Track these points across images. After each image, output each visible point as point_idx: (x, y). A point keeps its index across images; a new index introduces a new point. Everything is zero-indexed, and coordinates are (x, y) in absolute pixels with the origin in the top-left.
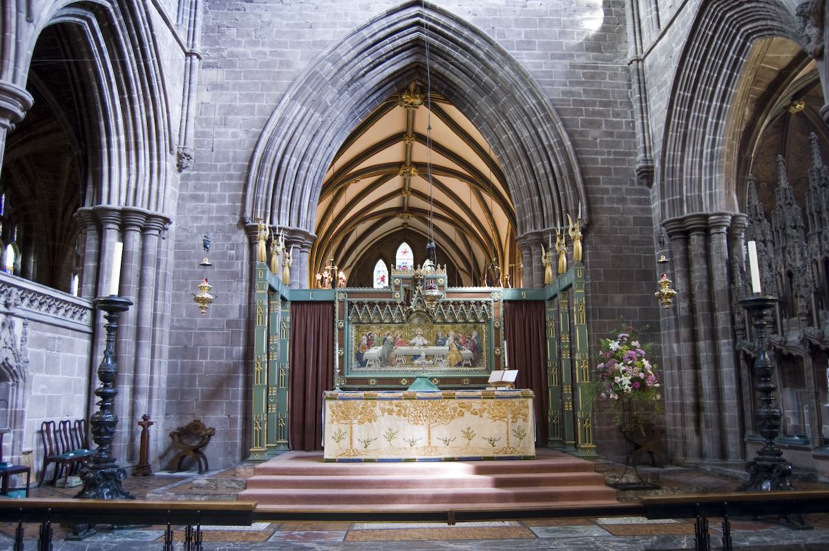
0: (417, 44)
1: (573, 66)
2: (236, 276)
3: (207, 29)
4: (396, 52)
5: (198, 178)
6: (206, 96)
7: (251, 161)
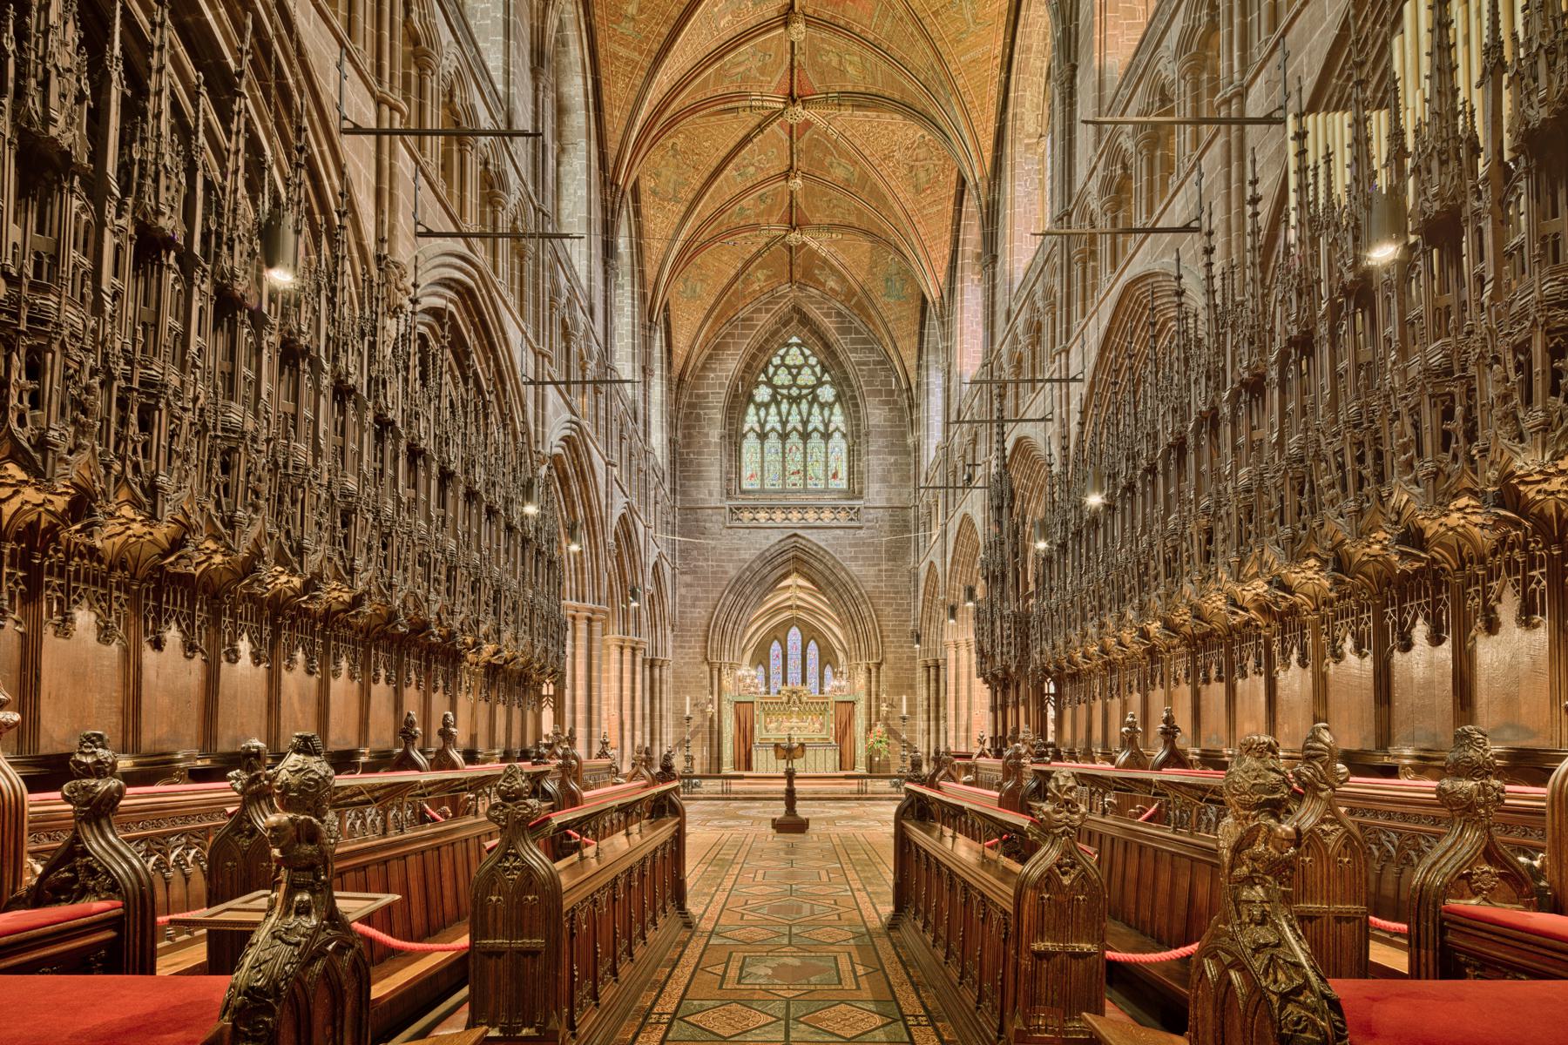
0: (795, 557)
1: (880, 571)
2: (703, 687)
3: (681, 551)
4: (784, 563)
5: (682, 636)
6: (683, 591)
7: (709, 627)
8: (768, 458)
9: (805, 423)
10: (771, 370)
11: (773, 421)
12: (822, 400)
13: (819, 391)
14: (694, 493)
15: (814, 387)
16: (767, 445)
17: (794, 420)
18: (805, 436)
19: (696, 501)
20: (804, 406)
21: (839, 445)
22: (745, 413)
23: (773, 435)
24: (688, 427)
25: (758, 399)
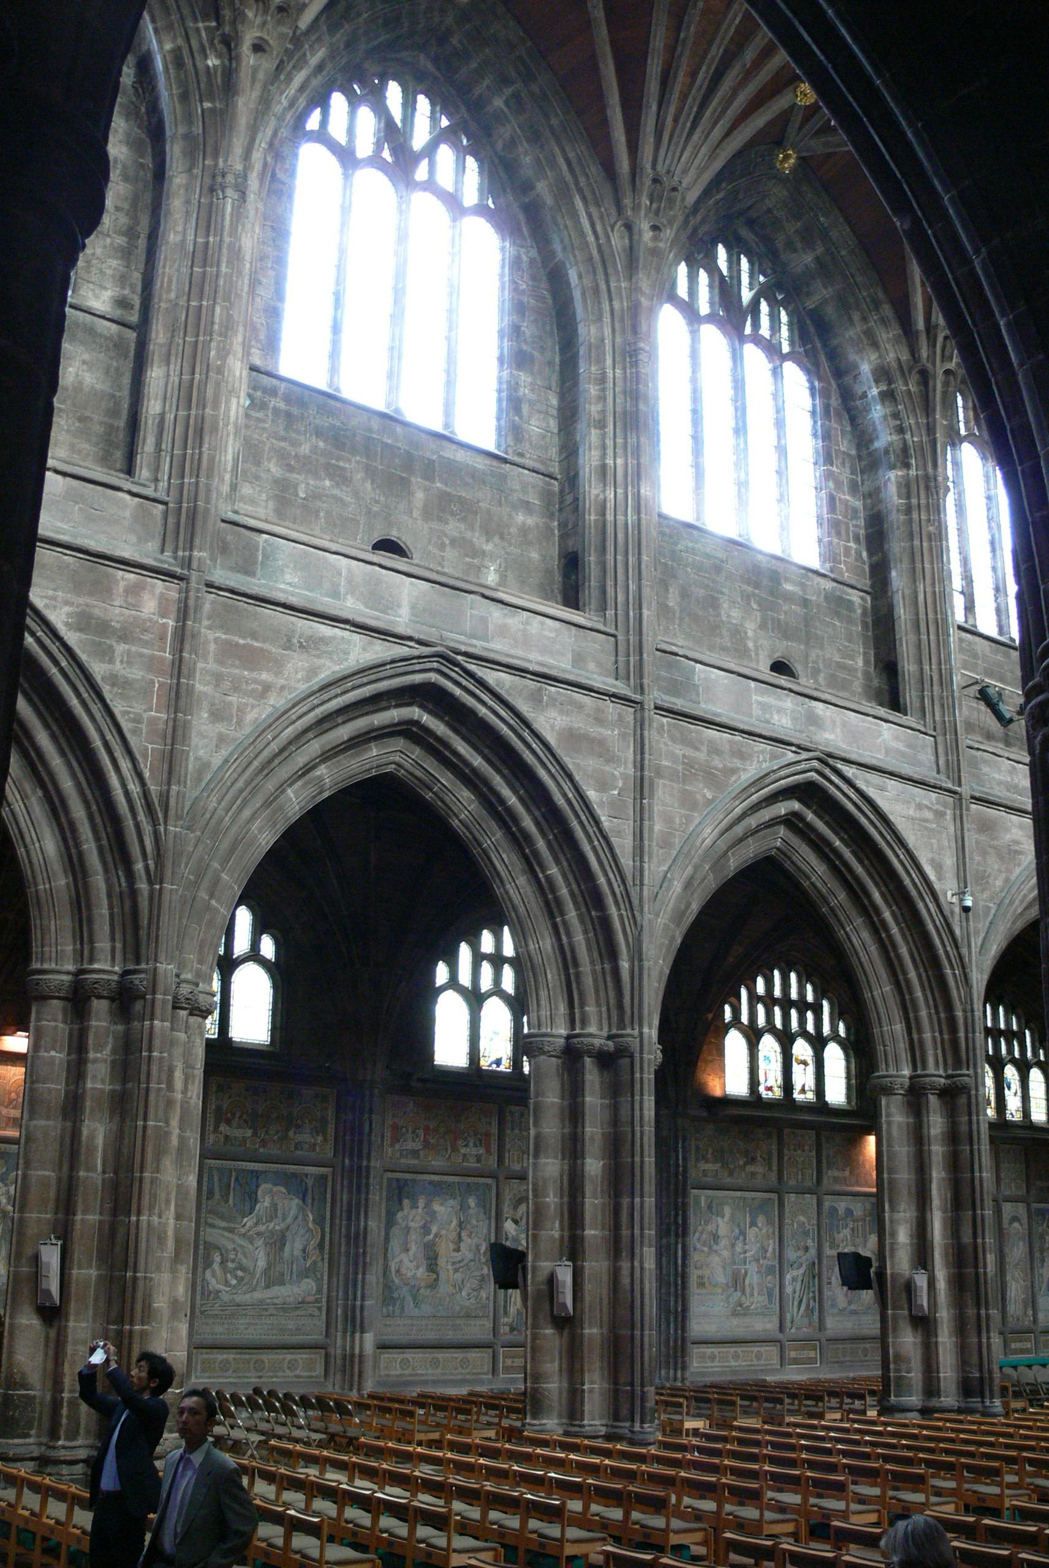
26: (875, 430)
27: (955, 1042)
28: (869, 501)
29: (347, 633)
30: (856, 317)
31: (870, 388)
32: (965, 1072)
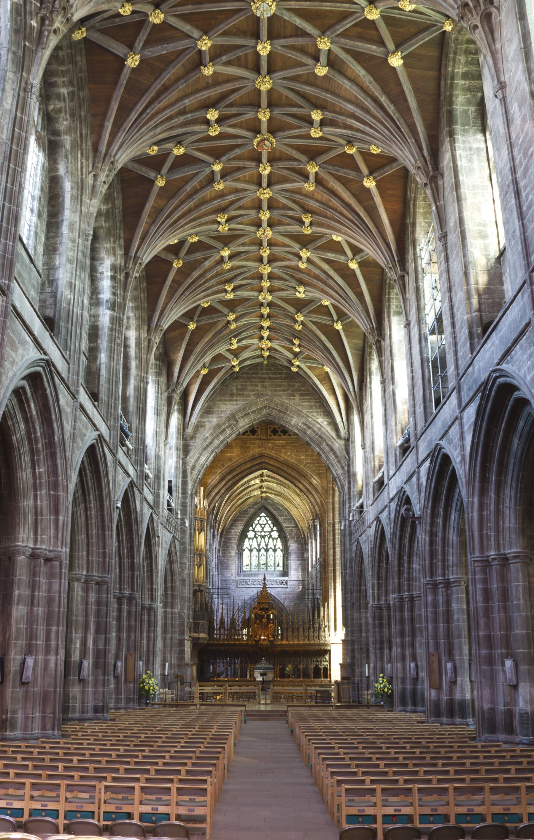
8: (253, 558)
9: (267, 545)
10: (254, 525)
11: (255, 545)
12: (273, 537)
13: (272, 534)
14: (226, 574)
15: (270, 532)
16: (253, 553)
17: (263, 545)
18: (267, 550)
19: (226, 577)
20: (266, 538)
21: (280, 554)
22: (244, 542)
23: (255, 550)
24: (223, 550)
25: (249, 536)
26: (103, 289)
27: (104, 562)
28: (93, 319)
29: (30, 341)
30: (112, 240)
31: (107, 271)
32: (107, 576)
